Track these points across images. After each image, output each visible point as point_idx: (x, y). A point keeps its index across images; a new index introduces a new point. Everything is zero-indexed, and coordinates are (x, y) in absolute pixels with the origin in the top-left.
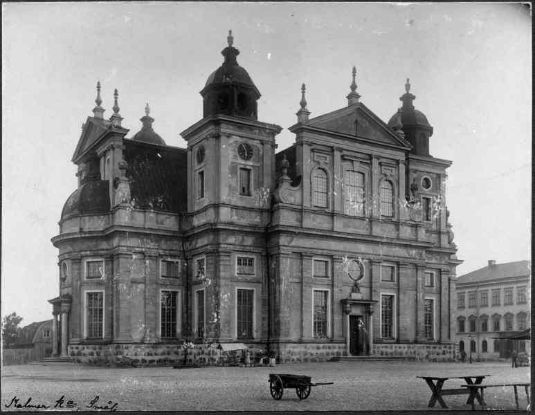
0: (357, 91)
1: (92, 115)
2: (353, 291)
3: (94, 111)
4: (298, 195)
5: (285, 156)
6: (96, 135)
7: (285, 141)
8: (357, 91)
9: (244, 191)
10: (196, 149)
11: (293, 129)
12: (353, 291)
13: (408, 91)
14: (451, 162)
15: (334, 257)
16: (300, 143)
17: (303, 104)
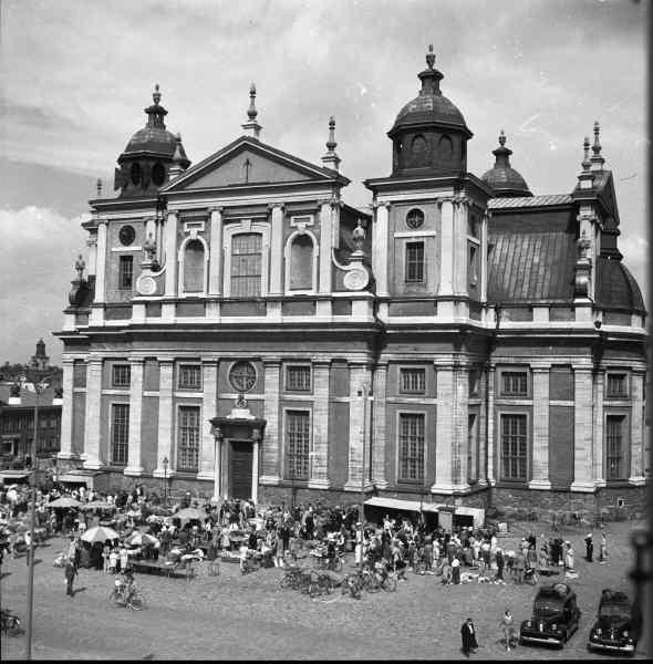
13: (431, 66)
15: (203, 359)
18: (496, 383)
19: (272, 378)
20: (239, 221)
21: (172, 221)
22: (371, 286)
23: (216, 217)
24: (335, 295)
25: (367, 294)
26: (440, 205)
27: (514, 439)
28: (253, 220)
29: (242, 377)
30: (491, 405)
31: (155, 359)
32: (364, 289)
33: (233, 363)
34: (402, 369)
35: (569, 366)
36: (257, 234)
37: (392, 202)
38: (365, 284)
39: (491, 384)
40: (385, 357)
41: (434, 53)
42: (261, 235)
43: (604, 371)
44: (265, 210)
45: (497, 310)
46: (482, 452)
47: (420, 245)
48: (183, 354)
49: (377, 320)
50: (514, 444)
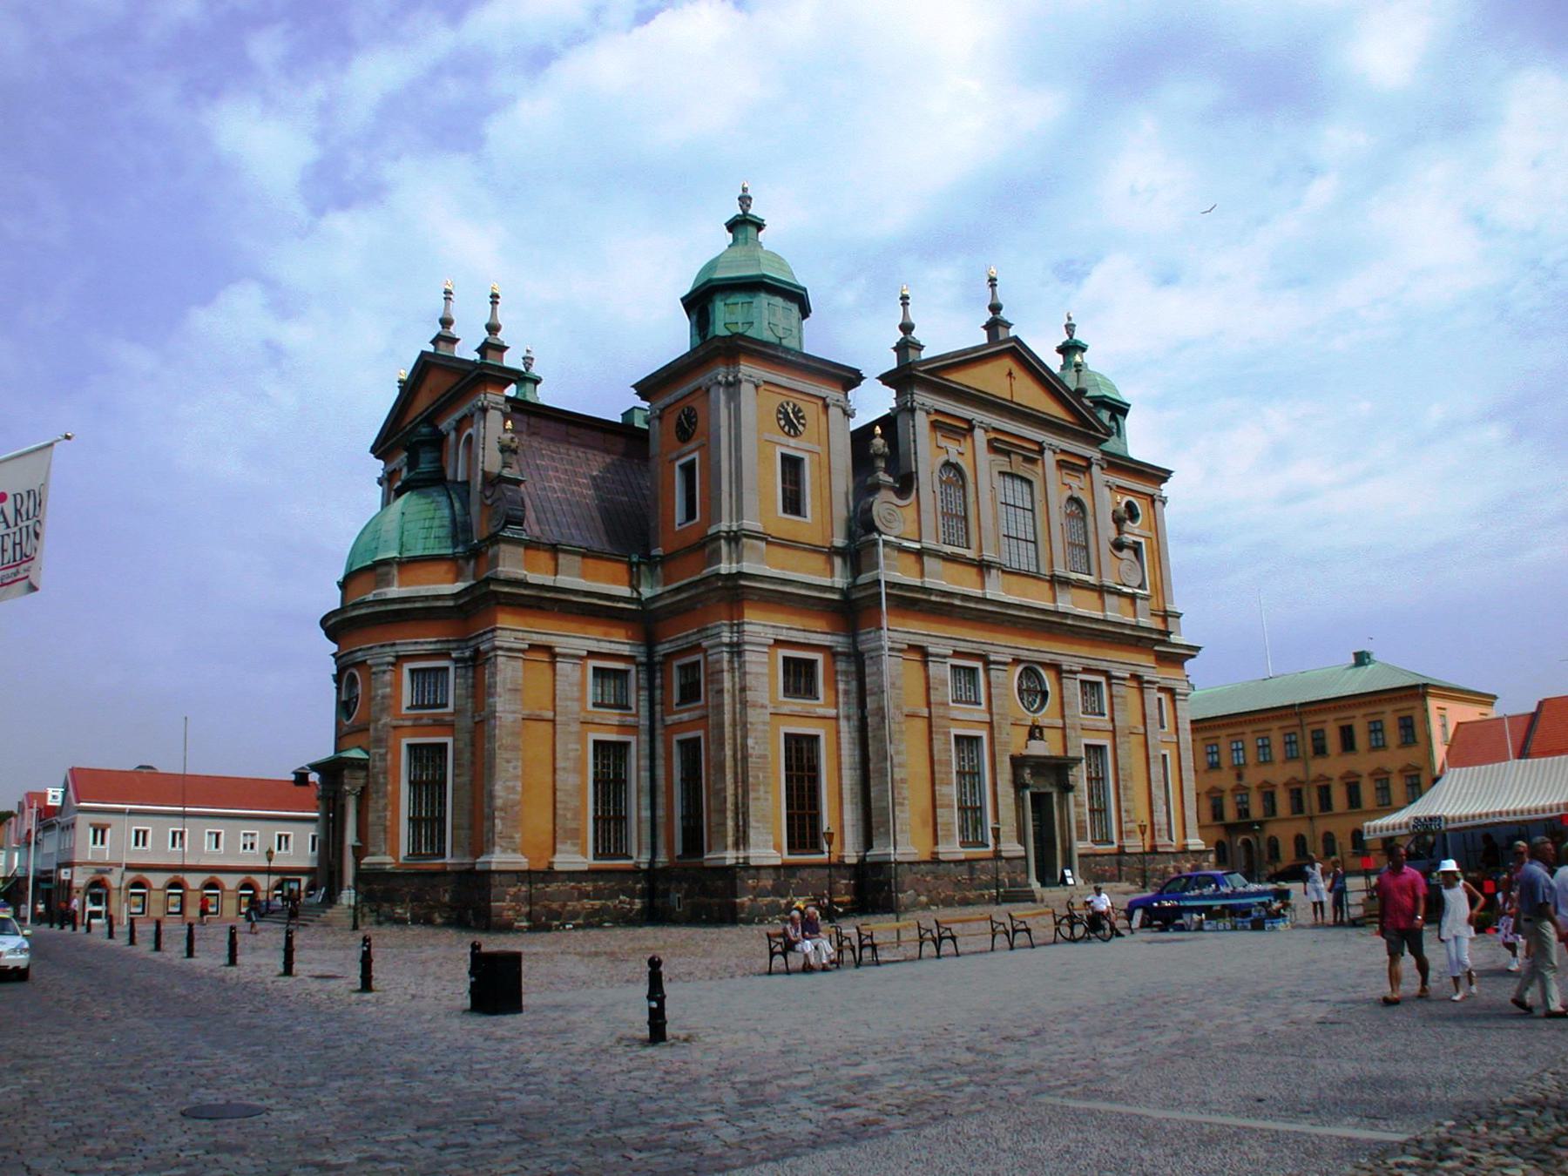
0: (1003, 314)
1: (431, 348)
2: (1031, 736)
3: (434, 342)
4: (911, 513)
5: (878, 430)
6: (437, 383)
7: (872, 402)
8: (1003, 314)
9: (793, 504)
10: (672, 421)
11: (887, 379)
12: (1031, 736)
14: (1169, 473)
16: (905, 409)
17: (907, 328)
19: (1073, 688)
20: (1008, 454)
33: (1020, 669)
37: (1118, 487)
38: (1139, 582)
41: (1073, 322)
42: (1030, 483)
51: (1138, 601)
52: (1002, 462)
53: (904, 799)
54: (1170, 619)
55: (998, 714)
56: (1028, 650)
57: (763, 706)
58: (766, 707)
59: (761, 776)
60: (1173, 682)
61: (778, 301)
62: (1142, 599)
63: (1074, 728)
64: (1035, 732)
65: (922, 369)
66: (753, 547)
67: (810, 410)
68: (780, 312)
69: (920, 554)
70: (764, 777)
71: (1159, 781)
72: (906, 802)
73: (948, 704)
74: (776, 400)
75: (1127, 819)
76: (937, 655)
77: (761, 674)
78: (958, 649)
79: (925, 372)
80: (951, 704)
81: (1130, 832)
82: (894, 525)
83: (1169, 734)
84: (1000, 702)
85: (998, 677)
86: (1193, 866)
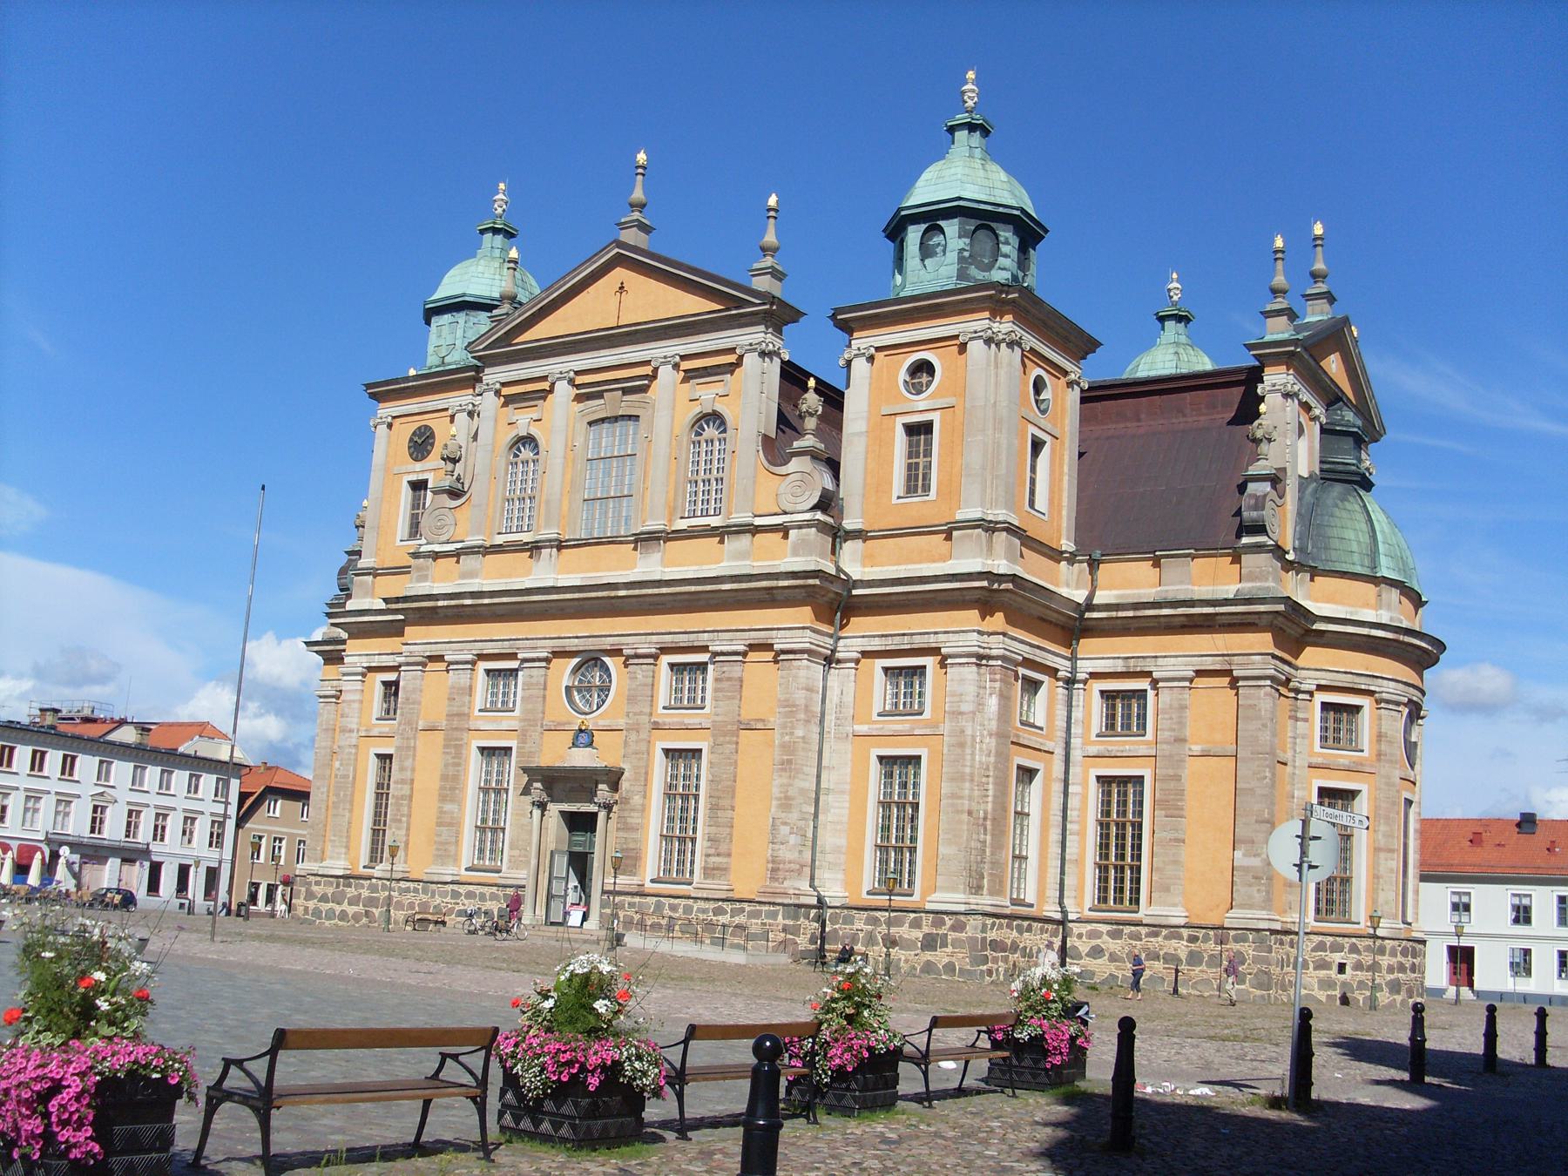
18: (1088, 714)
20: (599, 395)
21: (489, 403)
22: (827, 503)
23: (563, 390)
24: (758, 521)
25: (819, 515)
26: (963, 348)
27: (1121, 826)
28: (625, 391)
29: (589, 689)
30: (1076, 755)
31: (440, 658)
32: (814, 508)
33: (576, 660)
34: (886, 670)
35: (1228, 673)
36: (630, 417)
37: (878, 349)
38: (815, 500)
39: (1077, 714)
40: (849, 647)
43: (1311, 694)
44: (647, 370)
45: (1093, 565)
46: (1055, 850)
47: (927, 428)
48: (490, 649)
49: (839, 569)
50: (1121, 837)
51: (792, 533)
52: (597, 408)
53: (403, 815)
54: (955, 533)
55: (524, 720)
56: (577, 637)
57: (351, 731)
58: (351, 731)
59: (342, 793)
60: (932, 638)
61: (447, 318)
62: (800, 527)
63: (636, 728)
64: (584, 737)
65: (481, 347)
66: (362, 584)
67: (439, 425)
68: (445, 330)
69: (457, 554)
70: (345, 795)
71: (787, 798)
72: (404, 819)
73: (467, 716)
74: (405, 430)
75: (712, 851)
76: (457, 663)
77: (354, 701)
78: (485, 652)
79: (484, 349)
80: (477, 713)
81: (714, 869)
82: (445, 530)
83: (928, 724)
84: (530, 706)
85: (532, 677)
86: (926, 936)
